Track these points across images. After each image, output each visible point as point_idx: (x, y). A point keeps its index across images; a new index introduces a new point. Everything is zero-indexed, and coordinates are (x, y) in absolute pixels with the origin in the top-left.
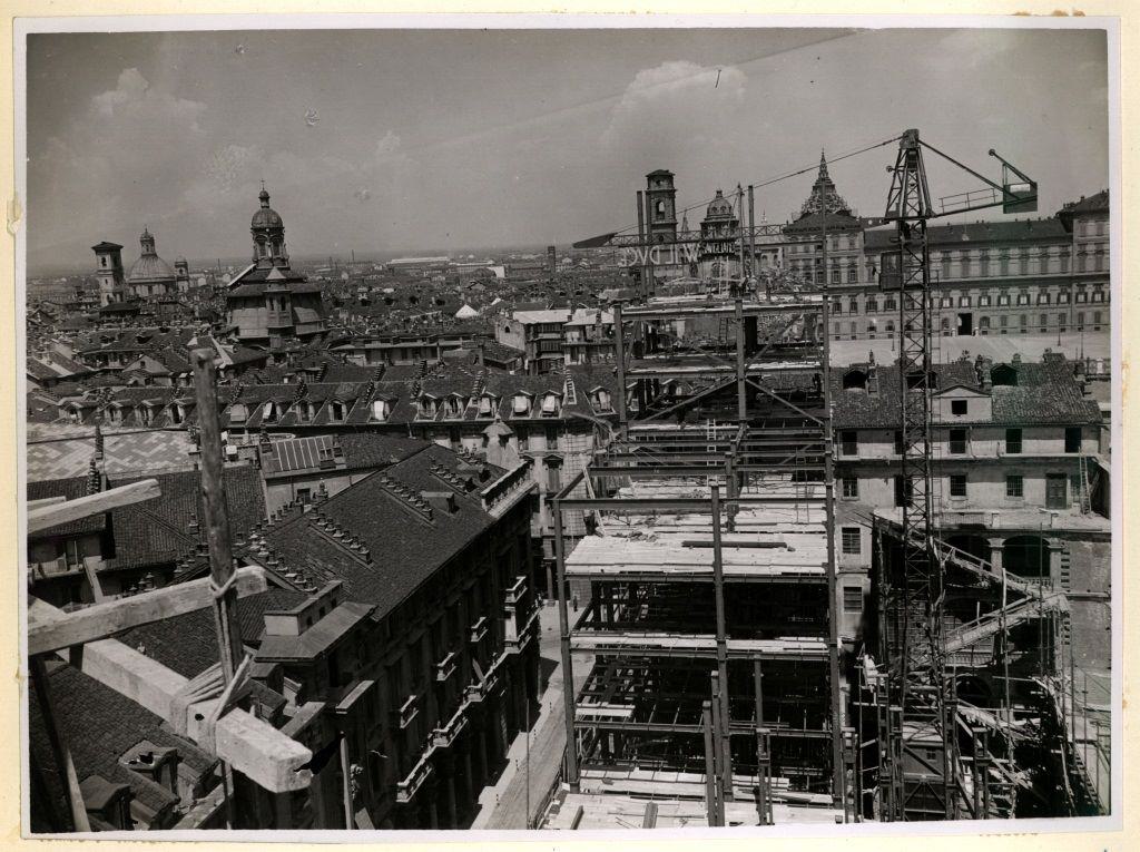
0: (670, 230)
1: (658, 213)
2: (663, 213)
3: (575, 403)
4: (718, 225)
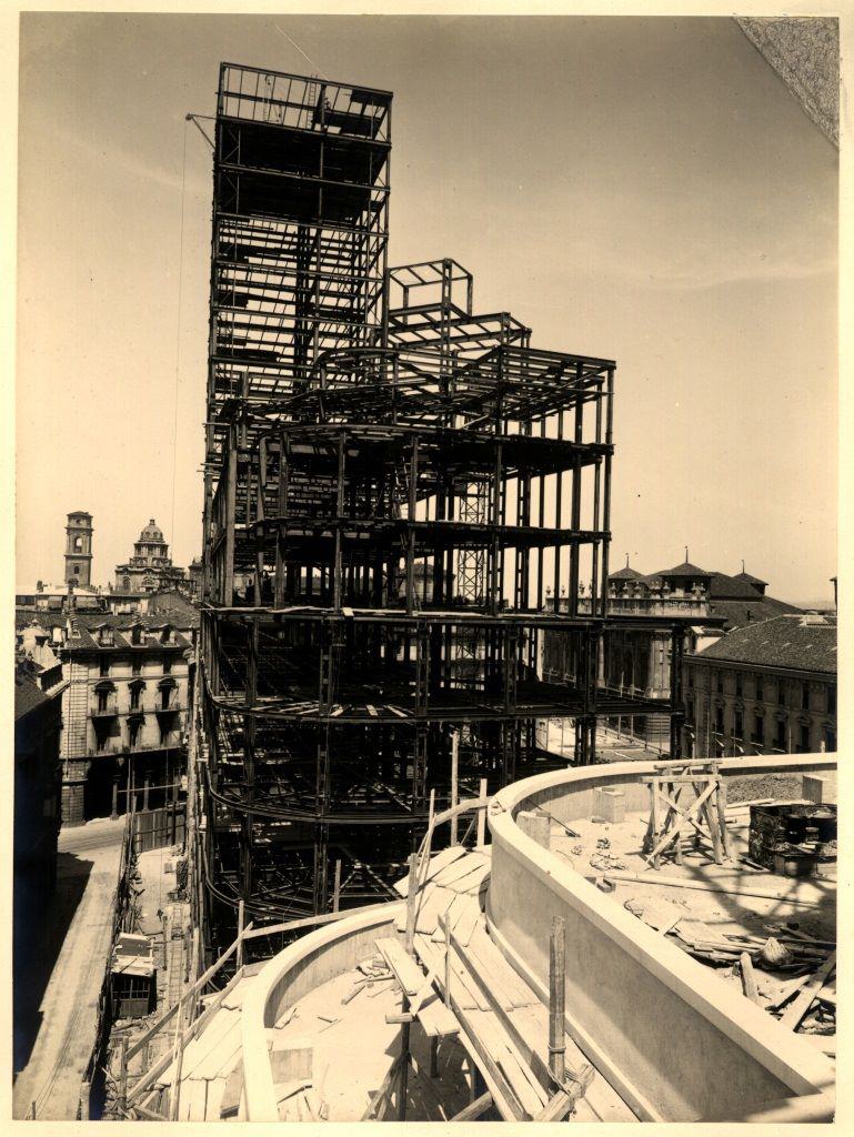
0: (86, 563)
1: (75, 546)
2: (80, 548)
3: (80, 637)
4: (151, 547)
